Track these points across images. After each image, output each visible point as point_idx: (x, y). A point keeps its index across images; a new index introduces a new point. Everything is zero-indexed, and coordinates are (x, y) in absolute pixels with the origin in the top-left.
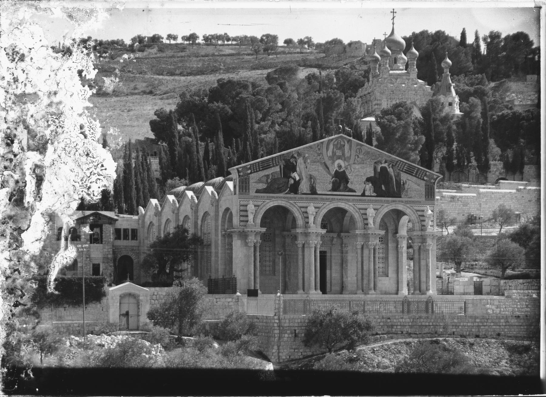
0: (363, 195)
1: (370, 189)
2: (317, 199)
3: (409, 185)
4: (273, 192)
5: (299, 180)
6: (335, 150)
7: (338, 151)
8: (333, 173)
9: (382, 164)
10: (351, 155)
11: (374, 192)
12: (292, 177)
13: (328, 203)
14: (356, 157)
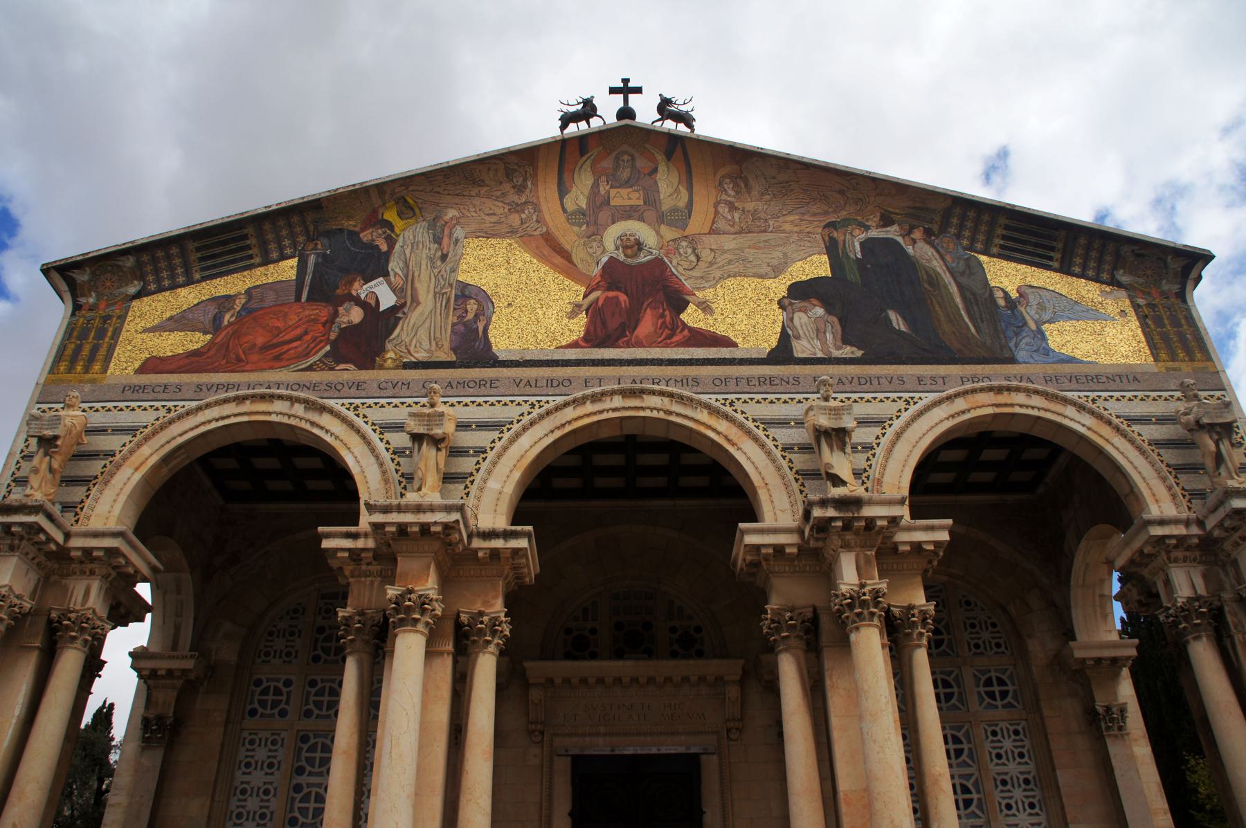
0: (782, 354)
1: (819, 333)
2: (492, 383)
3: (1042, 307)
4: (237, 365)
5: (393, 310)
7: (624, 192)
8: (596, 271)
9: (867, 228)
11: (846, 341)
12: (358, 301)
14: (724, 209)
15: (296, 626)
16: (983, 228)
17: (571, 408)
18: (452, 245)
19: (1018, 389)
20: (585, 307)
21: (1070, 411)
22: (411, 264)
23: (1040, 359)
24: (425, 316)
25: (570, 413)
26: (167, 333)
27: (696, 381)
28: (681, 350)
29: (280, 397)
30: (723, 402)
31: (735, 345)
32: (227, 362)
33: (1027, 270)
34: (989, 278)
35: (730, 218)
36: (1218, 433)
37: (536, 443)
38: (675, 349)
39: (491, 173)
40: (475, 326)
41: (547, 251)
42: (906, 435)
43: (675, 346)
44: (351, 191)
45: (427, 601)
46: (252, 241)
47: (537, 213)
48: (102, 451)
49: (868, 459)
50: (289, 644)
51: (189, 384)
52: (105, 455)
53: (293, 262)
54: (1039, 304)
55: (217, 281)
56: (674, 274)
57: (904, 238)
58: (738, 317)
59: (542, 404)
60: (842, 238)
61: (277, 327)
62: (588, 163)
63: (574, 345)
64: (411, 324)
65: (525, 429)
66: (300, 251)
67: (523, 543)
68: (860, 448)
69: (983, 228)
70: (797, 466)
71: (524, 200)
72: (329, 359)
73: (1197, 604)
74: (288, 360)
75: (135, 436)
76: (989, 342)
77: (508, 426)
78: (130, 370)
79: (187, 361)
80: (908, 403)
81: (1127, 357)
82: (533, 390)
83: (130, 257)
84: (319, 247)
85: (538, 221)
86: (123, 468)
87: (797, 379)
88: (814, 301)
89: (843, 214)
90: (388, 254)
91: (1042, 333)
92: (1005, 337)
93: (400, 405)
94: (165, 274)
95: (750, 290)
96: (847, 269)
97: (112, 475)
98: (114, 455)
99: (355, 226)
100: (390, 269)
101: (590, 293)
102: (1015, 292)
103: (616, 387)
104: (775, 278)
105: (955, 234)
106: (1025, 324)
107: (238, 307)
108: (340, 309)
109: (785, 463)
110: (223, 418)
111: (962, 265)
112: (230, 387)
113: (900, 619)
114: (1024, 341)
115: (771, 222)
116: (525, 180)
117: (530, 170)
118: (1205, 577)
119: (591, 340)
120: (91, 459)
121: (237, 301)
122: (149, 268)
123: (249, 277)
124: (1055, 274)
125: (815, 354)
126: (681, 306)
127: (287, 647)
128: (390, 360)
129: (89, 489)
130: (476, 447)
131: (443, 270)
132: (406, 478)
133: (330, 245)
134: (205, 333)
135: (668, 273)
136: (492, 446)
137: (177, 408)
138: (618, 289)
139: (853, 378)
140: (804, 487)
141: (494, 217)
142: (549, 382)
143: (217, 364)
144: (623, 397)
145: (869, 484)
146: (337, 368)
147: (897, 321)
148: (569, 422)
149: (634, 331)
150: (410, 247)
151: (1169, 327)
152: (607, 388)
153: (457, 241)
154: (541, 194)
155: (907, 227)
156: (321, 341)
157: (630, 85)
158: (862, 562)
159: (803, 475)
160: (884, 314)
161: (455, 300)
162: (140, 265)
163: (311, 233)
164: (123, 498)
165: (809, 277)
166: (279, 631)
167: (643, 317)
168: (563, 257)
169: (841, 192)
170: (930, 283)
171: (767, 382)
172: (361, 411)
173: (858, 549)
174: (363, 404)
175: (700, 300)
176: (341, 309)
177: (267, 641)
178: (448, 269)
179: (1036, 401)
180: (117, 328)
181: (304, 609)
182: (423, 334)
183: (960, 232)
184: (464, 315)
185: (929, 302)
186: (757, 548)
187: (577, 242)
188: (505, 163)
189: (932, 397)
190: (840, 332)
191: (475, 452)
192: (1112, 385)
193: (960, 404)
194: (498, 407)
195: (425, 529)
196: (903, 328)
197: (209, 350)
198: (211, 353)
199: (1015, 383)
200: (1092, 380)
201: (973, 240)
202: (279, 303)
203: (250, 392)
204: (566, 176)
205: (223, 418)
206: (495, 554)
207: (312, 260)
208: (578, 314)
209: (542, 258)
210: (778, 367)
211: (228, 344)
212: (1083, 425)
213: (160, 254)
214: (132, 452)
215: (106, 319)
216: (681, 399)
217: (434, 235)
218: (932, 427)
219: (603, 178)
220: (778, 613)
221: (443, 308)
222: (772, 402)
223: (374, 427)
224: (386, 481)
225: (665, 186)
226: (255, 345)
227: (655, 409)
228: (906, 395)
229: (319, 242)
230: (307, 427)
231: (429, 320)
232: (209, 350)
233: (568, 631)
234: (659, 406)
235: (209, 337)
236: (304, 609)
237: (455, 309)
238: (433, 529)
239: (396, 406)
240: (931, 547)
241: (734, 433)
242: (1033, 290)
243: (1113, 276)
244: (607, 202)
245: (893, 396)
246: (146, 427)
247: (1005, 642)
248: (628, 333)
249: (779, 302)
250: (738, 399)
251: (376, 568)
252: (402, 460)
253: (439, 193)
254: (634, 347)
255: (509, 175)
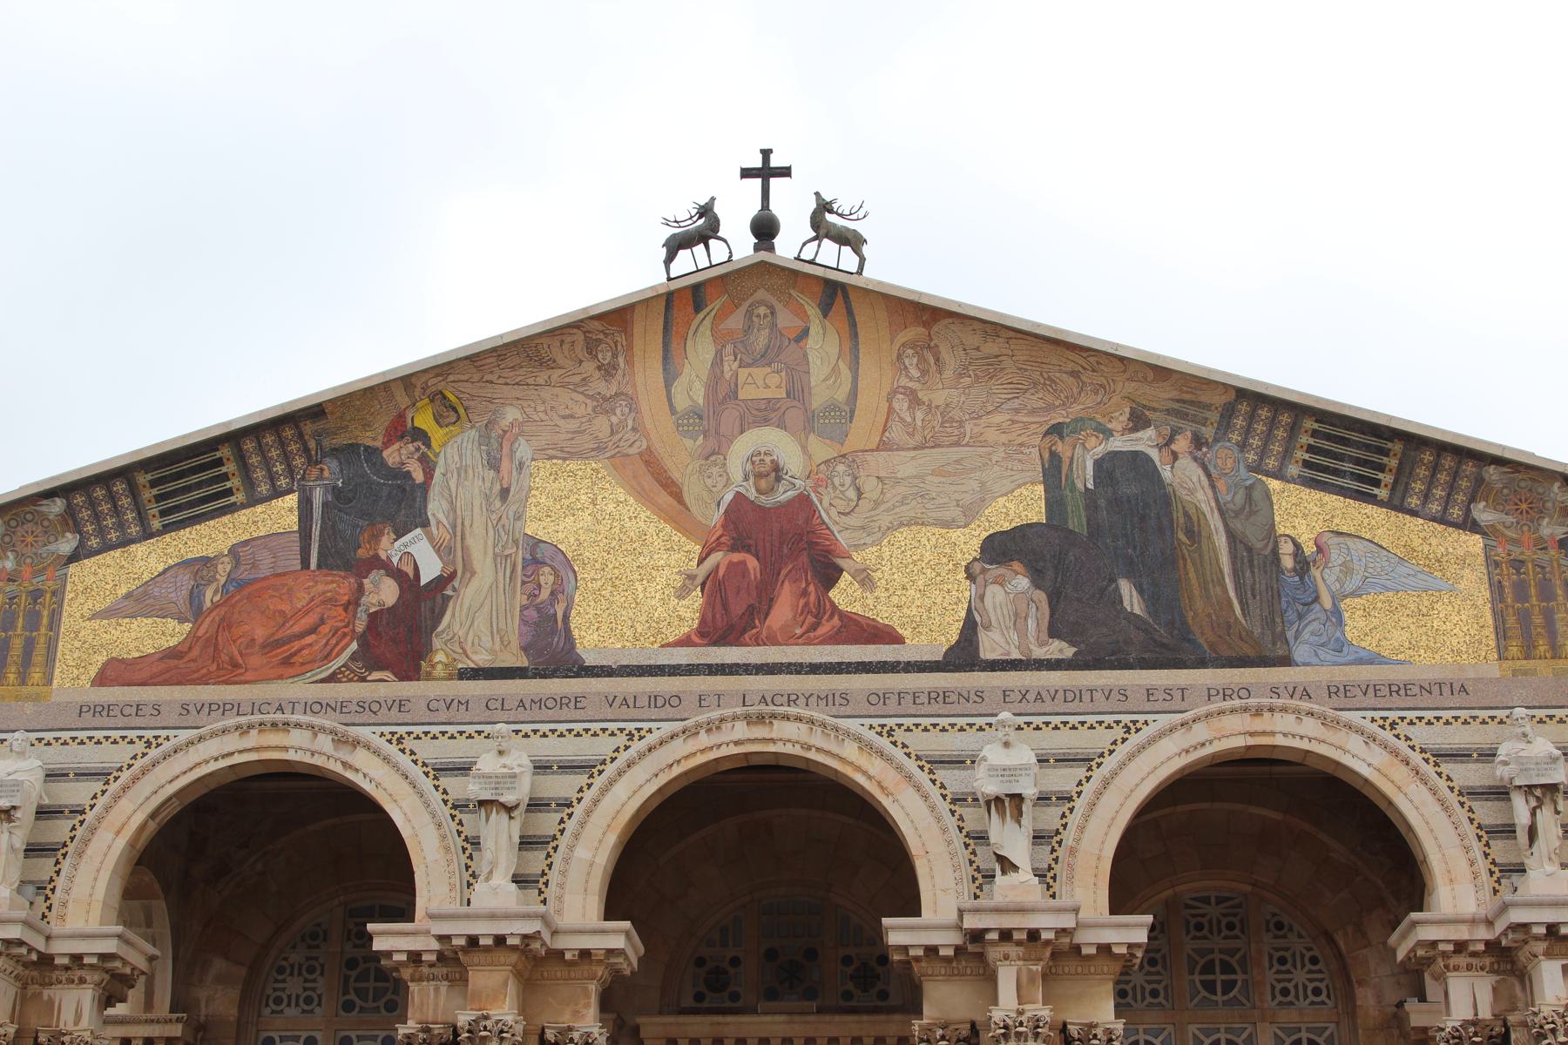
0: (963, 656)
1: (1018, 619)
3: (1347, 569)
4: (232, 672)
5: (442, 582)
6: (730, 365)
7: (759, 372)
8: (716, 517)
9: (1108, 433)
10: (854, 394)
11: (1054, 632)
13: (668, 728)
14: (901, 404)
15: (316, 959)
16: (1280, 433)
17: (679, 741)
18: (514, 473)
19: (1284, 710)
20: (700, 580)
21: (1355, 743)
22: (458, 504)
23: (1329, 657)
24: (483, 595)
25: (680, 748)
26: (127, 620)
27: (845, 697)
28: (829, 648)
29: (298, 725)
30: (879, 729)
31: (897, 639)
32: (218, 668)
33: (1337, 504)
34: (1277, 519)
35: (909, 419)
36: (1538, 798)
37: (635, 792)
38: (820, 648)
39: (566, 347)
40: (552, 611)
41: (649, 482)
42: (1117, 780)
43: (821, 643)
44: (365, 390)
45: (506, 1029)
46: (230, 467)
47: (633, 414)
48: (66, 806)
49: (1063, 816)
50: (308, 985)
51: (170, 702)
52: (71, 812)
53: (292, 500)
54: (1343, 564)
55: (185, 533)
56: (824, 523)
57: (1160, 447)
58: (908, 593)
59: (643, 733)
60: (1069, 454)
61: (282, 613)
62: (707, 322)
63: (685, 642)
64: (466, 606)
65: (620, 773)
66: (299, 480)
67: (618, 942)
68: (1054, 799)
69: (1280, 433)
70: (969, 826)
71: (614, 389)
72: (360, 664)
73: (1472, 1029)
74: (302, 664)
75: (107, 783)
76: (1257, 631)
77: (599, 767)
78: (85, 680)
79: (162, 666)
80: (1128, 731)
81: (1459, 652)
82: (633, 713)
83: (57, 499)
84: (326, 474)
85: (634, 429)
86: (99, 831)
87: (980, 694)
88: (1016, 565)
89: (1076, 408)
90: (425, 487)
91: (1337, 613)
92: (1283, 623)
93: (457, 735)
94: (109, 522)
95: (928, 547)
96: (1069, 508)
97: (86, 842)
98: (83, 812)
99: (374, 439)
100: (429, 514)
101: (708, 555)
102: (1312, 542)
103: (739, 710)
104: (965, 526)
105: (1237, 444)
106: (1317, 599)
107: (222, 582)
108: (366, 581)
109: (951, 822)
110: (223, 757)
111: (1240, 498)
112: (228, 707)
113: (1079, 1040)
114: (1309, 628)
115: (968, 427)
116: (615, 356)
117: (621, 339)
118: (1494, 989)
119: (708, 633)
120: (53, 818)
121: (220, 567)
122: (85, 514)
123: (231, 525)
124: (1380, 510)
125: (1009, 654)
126: (829, 574)
127: (305, 989)
128: (440, 667)
129: (57, 863)
130: (560, 798)
131: (504, 517)
132: (472, 844)
133: (341, 470)
134: (182, 620)
135: (816, 521)
136: (579, 796)
137: (160, 741)
138: (747, 549)
139: (1056, 691)
140: (976, 855)
141: (573, 421)
142: (652, 699)
143: (205, 671)
144: (748, 724)
145: (1061, 852)
146: (369, 678)
147: (1130, 598)
148: (679, 762)
149: (766, 618)
150: (455, 475)
151: (1534, 601)
152: (727, 712)
153: (521, 465)
154: (639, 378)
155: (1167, 431)
156: (345, 635)
157: (775, 162)
158: (1024, 979)
159: (974, 838)
160: (1114, 586)
161: (524, 568)
162: (70, 512)
163: (313, 453)
164: (105, 876)
165: (1014, 525)
166: (292, 966)
167: (779, 595)
168: (671, 494)
169: (1075, 374)
170: (1190, 533)
171: (940, 699)
172: (409, 743)
173: (1021, 963)
174: (409, 734)
175: (858, 566)
176: (366, 581)
177: (276, 981)
178: (511, 514)
179: (1310, 727)
180: (54, 610)
181: (325, 932)
182: (481, 623)
183: (1246, 438)
184: (537, 592)
185: (1181, 562)
186: (905, 948)
187: (690, 467)
188: (585, 333)
189: (1164, 720)
190: (1047, 618)
191: (558, 805)
192: (1426, 700)
193: (1200, 732)
194: (586, 737)
195: (500, 940)
196: (1137, 611)
197: (190, 648)
198: (195, 652)
199: (1279, 702)
200: (1397, 692)
201: (1263, 453)
202: (280, 571)
203: (257, 718)
204: (675, 345)
205: (223, 757)
206: (585, 954)
207: (318, 497)
208: (690, 591)
209: (643, 497)
210: (957, 674)
211: (216, 638)
212: (1369, 765)
213: (99, 493)
214: (108, 809)
215: (36, 595)
216: (824, 725)
217: (488, 454)
218: (1156, 768)
219: (729, 348)
220: (929, 1029)
221: (508, 580)
222: (944, 730)
223: (425, 769)
224: (447, 849)
225: (819, 362)
226: (253, 640)
227: (789, 741)
228: (1126, 718)
229: (325, 467)
230: (338, 768)
231: (488, 602)
232: (190, 648)
233: (700, 962)
234: (794, 737)
235: (187, 627)
236: (325, 932)
237: (524, 583)
238: (510, 941)
239: (452, 737)
240: (1124, 950)
241: (890, 777)
242: (1341, 539)
243: (1468, 511)
244: (737, 392)
245: (1109, 719)
246: (120, 769)
247: (1327, 987)
248: (757, 622)
249: (967, 569)
250: (900, 726)
251: (441, 971)
252: (465, 817)
253: (492, 382)
254: (765, 644)
255: (591, 348)
